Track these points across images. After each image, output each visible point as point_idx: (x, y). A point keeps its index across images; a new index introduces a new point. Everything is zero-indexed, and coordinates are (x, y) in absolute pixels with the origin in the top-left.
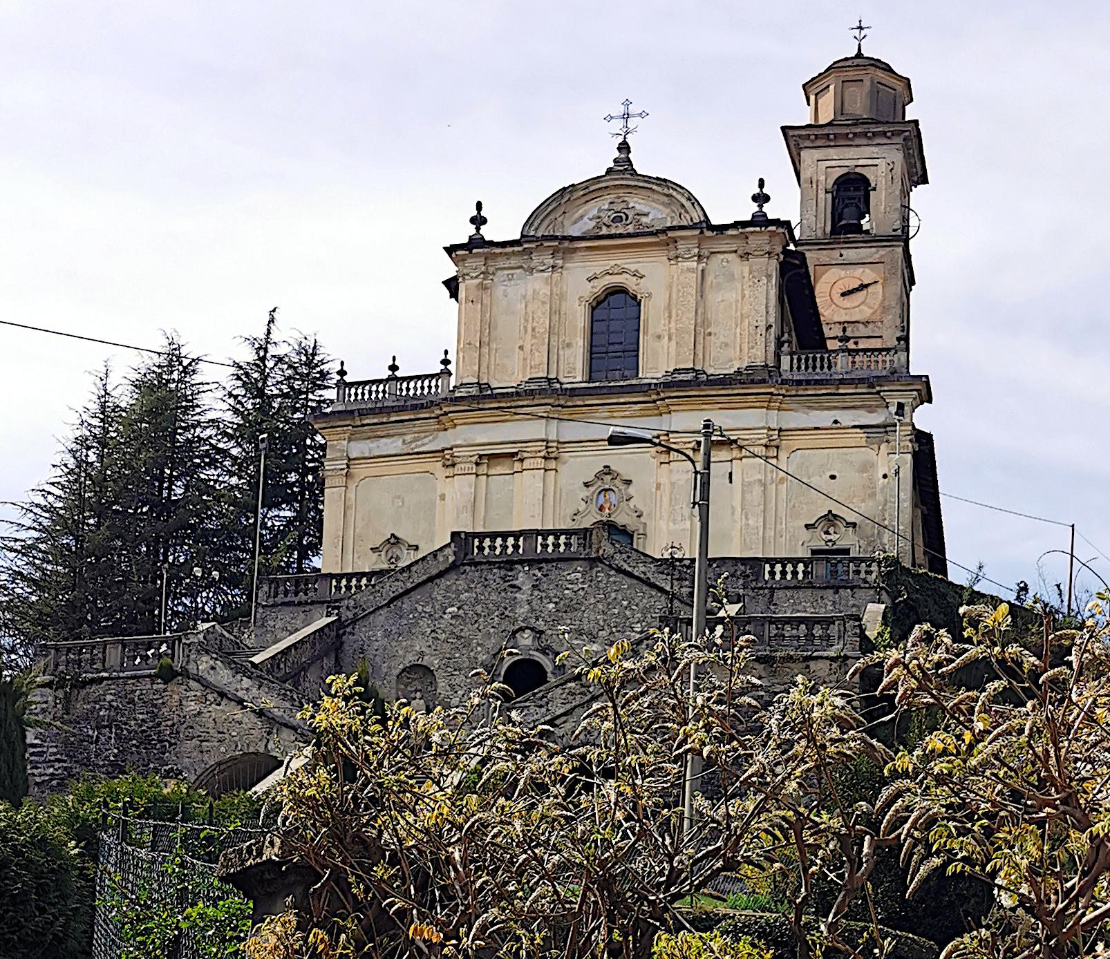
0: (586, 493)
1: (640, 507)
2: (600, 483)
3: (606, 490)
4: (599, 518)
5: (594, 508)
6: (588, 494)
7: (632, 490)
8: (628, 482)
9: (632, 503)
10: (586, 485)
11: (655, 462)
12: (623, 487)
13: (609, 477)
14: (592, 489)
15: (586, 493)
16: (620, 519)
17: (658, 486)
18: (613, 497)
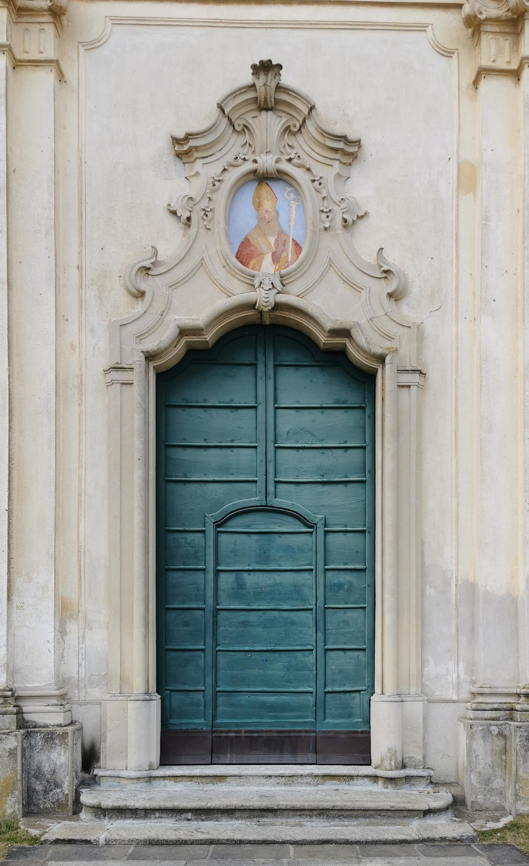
0: (175, 185)
1: (394, 259)
2: (234, 145)
3: (262, 178)
4: (241, 294)
5: (217, 248)
6: (196, 188)
7: (362, 187)
8: (346, 149)
9: (366, 243)
10: (185, 149)
11: (454, 73)
12: (328, 172)
13: (269, 125)
14: (206, 170)
15: (175, 185)
16: (328, 304)
17: (467, 178)
18: (287, 210)
